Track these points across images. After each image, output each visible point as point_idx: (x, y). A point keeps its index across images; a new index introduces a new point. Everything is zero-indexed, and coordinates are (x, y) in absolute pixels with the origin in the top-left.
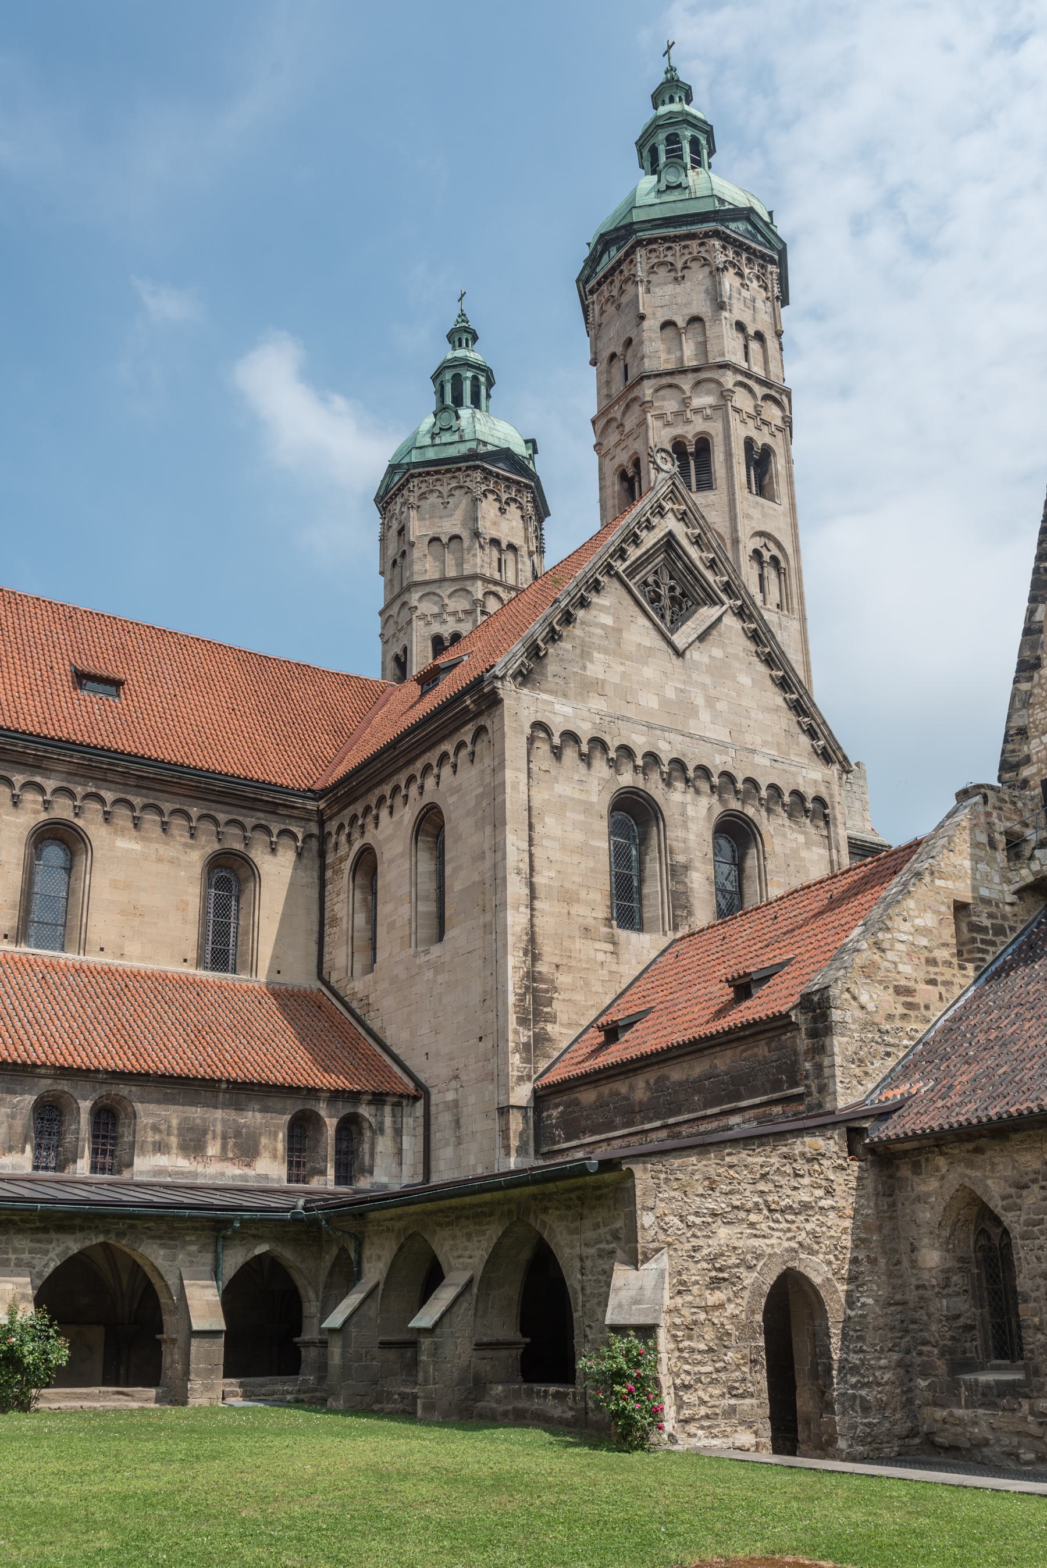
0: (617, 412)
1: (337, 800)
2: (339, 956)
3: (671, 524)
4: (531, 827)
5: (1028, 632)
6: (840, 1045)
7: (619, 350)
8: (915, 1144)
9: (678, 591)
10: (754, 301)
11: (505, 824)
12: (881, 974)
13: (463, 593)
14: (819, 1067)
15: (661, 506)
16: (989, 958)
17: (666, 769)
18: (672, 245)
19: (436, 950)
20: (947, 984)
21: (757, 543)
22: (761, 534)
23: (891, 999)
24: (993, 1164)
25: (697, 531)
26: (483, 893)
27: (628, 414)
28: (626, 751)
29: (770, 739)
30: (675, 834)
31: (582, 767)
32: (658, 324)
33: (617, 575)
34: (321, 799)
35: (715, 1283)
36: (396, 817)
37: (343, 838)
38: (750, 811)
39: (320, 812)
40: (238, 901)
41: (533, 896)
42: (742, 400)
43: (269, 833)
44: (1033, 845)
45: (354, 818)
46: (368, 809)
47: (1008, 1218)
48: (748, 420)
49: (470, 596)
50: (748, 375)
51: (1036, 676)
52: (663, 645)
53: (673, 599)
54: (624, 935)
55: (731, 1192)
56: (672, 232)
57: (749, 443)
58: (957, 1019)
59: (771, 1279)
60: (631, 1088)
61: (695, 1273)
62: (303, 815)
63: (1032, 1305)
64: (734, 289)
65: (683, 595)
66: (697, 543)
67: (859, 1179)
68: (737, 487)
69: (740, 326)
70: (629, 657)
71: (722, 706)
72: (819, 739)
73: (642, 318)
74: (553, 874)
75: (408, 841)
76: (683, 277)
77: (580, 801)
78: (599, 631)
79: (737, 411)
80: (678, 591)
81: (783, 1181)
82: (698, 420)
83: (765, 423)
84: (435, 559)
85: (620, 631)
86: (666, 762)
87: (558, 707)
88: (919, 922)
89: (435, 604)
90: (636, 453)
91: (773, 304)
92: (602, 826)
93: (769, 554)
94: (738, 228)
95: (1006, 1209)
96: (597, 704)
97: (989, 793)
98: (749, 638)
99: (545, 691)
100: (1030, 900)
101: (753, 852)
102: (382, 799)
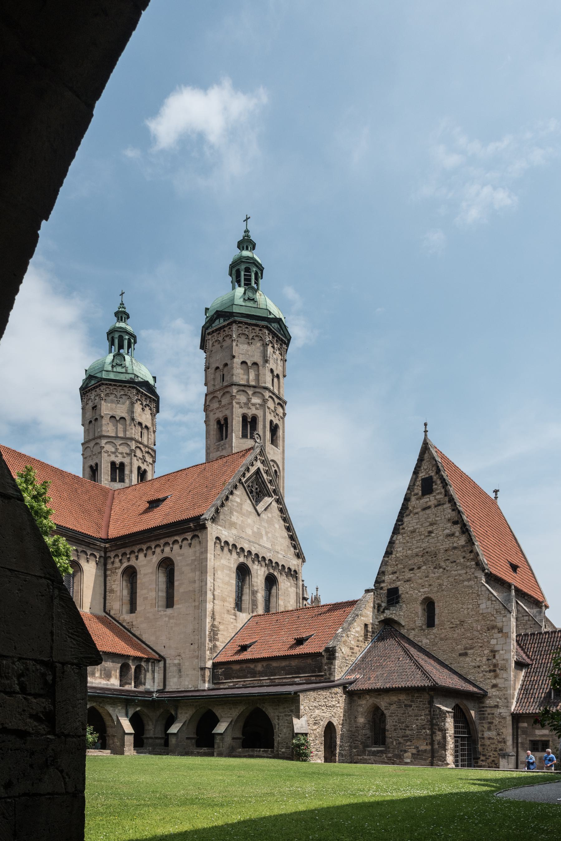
1: (116, 545)
5: (390, 543)
6: (337, 663)
8: (360, 692)
9: (258, 490)
10: (277, 361)
11: (207, 573)
12: (347, 643)
13: (126, 445)
14: (330, 668)
15: (257, 457)
17: (253, 557)
18: (248, 327)
23: (349, 651)
24: (383, 698)
25: (267, 468)
26: (194, 595)
27: (224, 397)
28: (242, 549)
29: (282, 548)
31: (229, 554)
32: (240, 362)
33: (242, 482)
34: (107, 543)
36: (148, 558)
40: (73, 579)
43: (86, 554)
44: (383, 608)
47: (385, 712)
48: (272, 413)
49: (129, 447)
50: (274, 394)
51: (390, 556)
52: (254, 511)
53: (256, 492)
55: (319, 701)
56: (249, 321)
59: (326, 723)
61: (311, 721)
62: (99, 548)
63: (389, 732)
64: (271, 354)
65: (260, 491)
66: (266, 473)
67: (345, 699)
68: (266, 441)
70: (244, 515)
71: (270, 535)
72: (297, 550)
75: (155, 569)
76: (252, 343)
77: (228, 566)
78: (235, 504)
79: (269, 408)
80: (258, 490)
81: (329, 699)
82: (253, 408)
83: (277, 415)
84: (114, 426)
85: (242, 504)
86: (253, 554)
87: (223, 532)
88: (357, 629)
89: (113, 447)
90: (226, 415)
91: (284, 363)
93: (274, 469)
95: (385, 709)
96: (234, 531)
97: (375, 592)
98: (279, 511)
99: (221, 526)
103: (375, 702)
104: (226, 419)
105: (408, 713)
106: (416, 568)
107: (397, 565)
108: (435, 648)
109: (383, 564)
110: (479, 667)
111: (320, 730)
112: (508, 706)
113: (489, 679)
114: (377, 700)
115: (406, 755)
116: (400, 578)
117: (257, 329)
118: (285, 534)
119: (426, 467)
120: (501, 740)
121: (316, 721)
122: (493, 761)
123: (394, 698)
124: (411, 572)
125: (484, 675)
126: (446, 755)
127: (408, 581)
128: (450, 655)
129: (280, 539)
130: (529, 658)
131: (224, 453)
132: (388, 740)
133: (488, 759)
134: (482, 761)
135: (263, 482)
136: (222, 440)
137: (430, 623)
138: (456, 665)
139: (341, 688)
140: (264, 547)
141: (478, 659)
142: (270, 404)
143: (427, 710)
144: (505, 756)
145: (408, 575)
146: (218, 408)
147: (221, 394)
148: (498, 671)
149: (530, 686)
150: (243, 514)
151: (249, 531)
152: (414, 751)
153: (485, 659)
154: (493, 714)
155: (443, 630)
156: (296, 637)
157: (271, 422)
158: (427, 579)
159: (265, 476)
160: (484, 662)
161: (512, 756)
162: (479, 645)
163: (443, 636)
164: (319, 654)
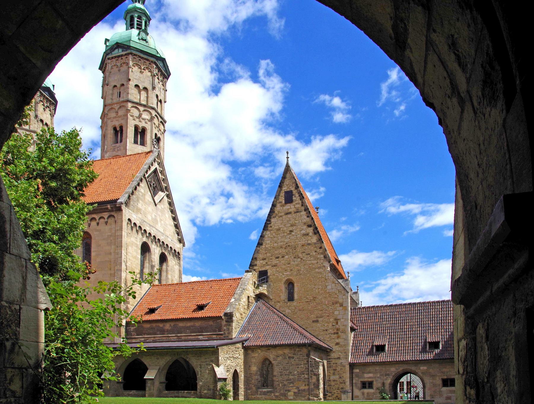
5: (261, 236)
6: (234, 324)
9: (155, 185)
14: (229, 329)
25: (162, 169)
27: (120, 110)
28: (145, 231)
30: (153, 256)
32: (134, 85)
47: (273, 362)
53: (154, 187)
56: (142, 55)
57: (156, 134)
60: (164, 326)
69: (157, 96)
80: (155, 185)
82: (143, 122)
90: (121, 124)
92: (139, 251)
94: (160, 64)
103: (265, 355)
104: (121, 127)
105: (291, 363)
106: (280, 257)
107: (266, 253)
108: (295, 316)
109: (256, 252)
110: (326, 330)
112: (347, 358)
113: (333, 339)
114: (267, 353)
115: (289, 393)
116: (269, 263)
117: (148, 63)
119: (287, 183)
120: (342, 381)
122: (337, 396)
123: (280, 352)
124: (277, 259)
125: (330, 336)
126: (319, 393)
127: (274, 266)
128: (306, 321)
129: (169, 226)
130: (354, 325)
131: (119, 153)
132: (276, 383)
133: (333, 395)
134: (329, 396)
135: (158, 180)
136: (117, 143)
137: (291, 298)
138: (310, 328)
139: (241, 343)
140: (159, 231)
141: (326, 325)
142: (156, 121)
143: (306, 360)
144: (345, 392)
145: (275, 261)
146: (115, 117)
147: (118, 107)
148: (340, 333)
149: (358, 344)
150: (146, 203)
151: (150, 218)
152: (296, 391)
153: (330, 325)
154: (337, 363)
155: (301, 304)
156: (198, 304)
158: (289, 265)
160: (330, 327)
161: (350, 392)
162: (327, 314)
163: (301, 308)
164: (220, 318)
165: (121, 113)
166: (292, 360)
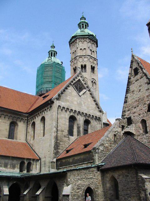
0: (74, 60)
2: (29, 138)
3: (80, 78)
4: (57, 121)
7: (74, 52)
16: (119, 143)
19: (43, 138)
20: (113, 146)
21: (92, 80)
22: (93, 79)
35: (78, 189)
36: (39, 117)
37: (30, 120)
38: (89, 119)
39: (27, 116)
41: (57, 131)
42: (91, 60)
45: (32, 117)
46: (34, 116)
50: (92, 57)
54: (70, 137)
58: (114, 152)
61: (75, 187)
62: (25, 116)
63: (120, 192)
65: (81, 88)
66: (83, 81)
73: (77, 48)
74: (60, 128)
78: (69, 93)
92: (68, 121)
95: (118, 179)
96: (68, 103)
100: (124, 134)
101: (89, 126)
102: (36, 115)
104: (76, 67)
111: (81, 192)
118: (94, 103)
121: (79, 187)
123: (121, 172)
132: (120, 197)
135: (82, 84)
145: (134, 110)
157: (92, 66)
159: (83, 82)
165: (75, 62)
166: (128, 178)
